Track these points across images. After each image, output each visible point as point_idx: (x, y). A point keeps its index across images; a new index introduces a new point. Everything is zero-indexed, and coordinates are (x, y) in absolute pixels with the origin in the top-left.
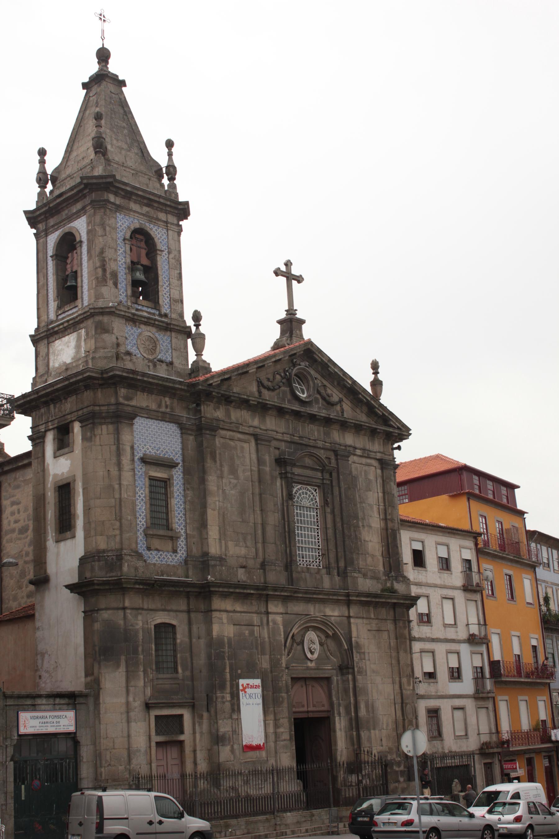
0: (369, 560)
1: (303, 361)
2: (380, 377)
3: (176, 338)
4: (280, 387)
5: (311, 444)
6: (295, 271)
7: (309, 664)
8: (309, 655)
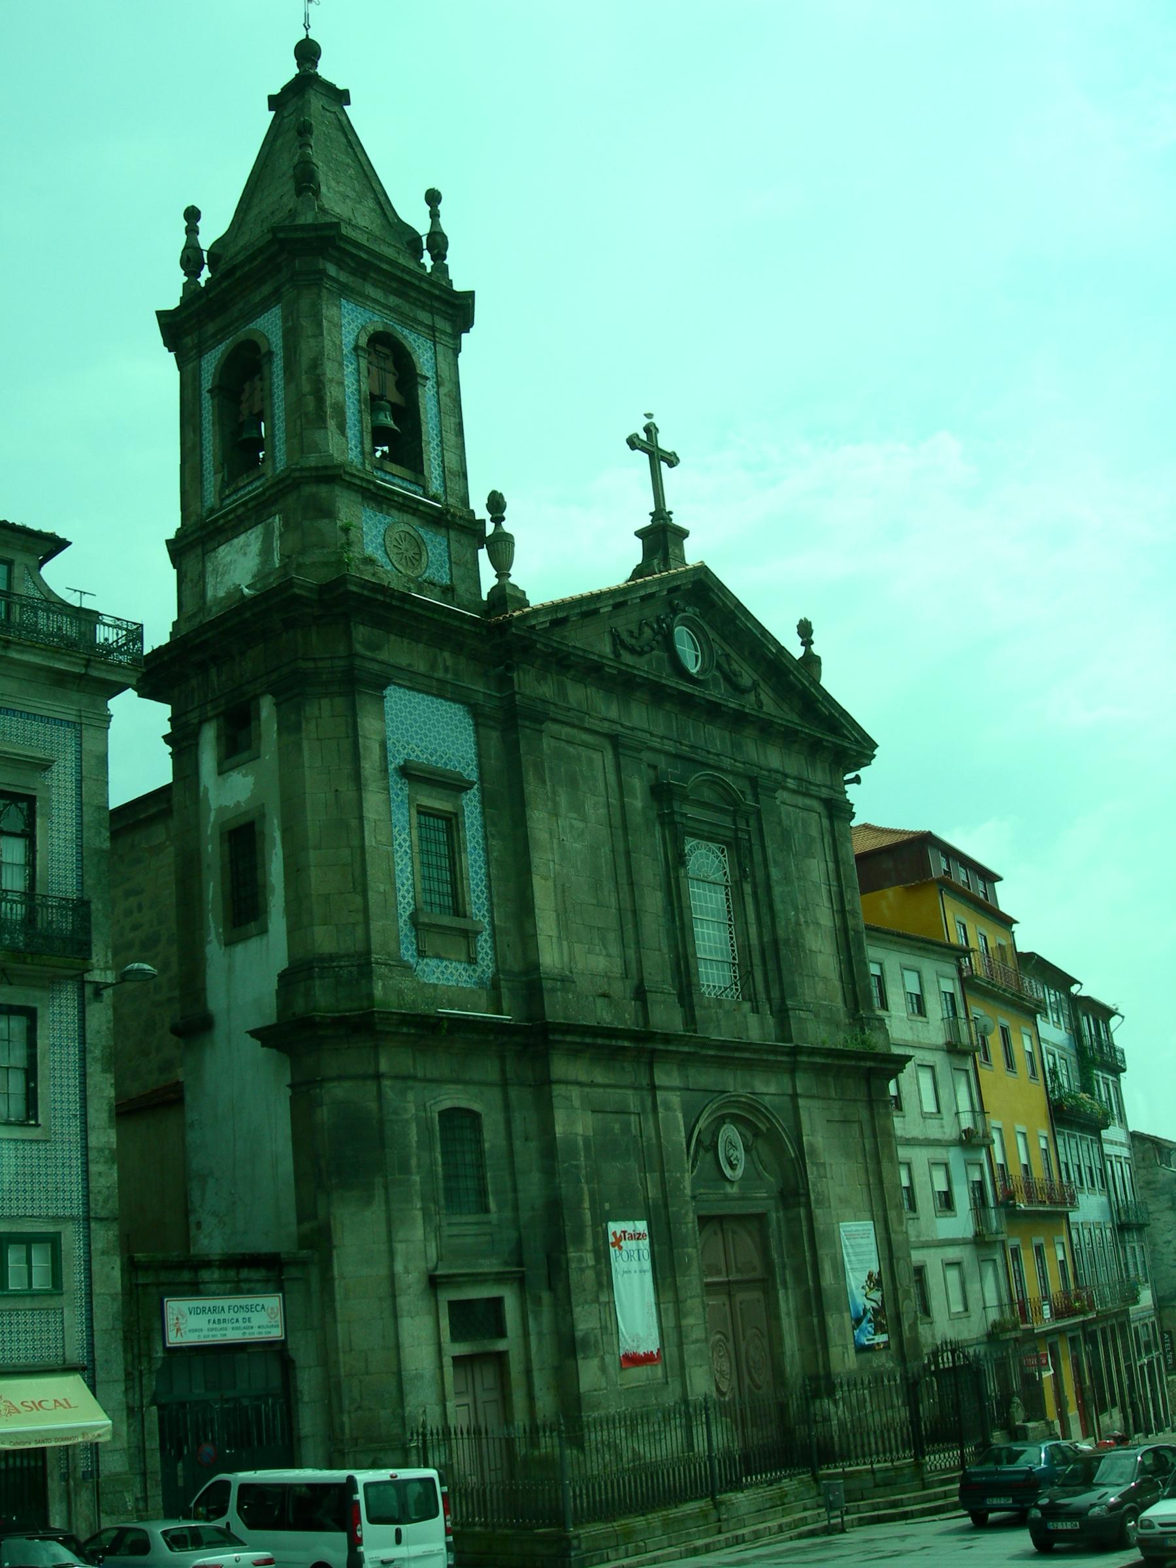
0: (820, 986)
1: (689, 605)
2: (815, 649)
3: (458, 541)
4: (652, 649)
5: (712, 762)
6: (665, 443)
8: (728, 1172)
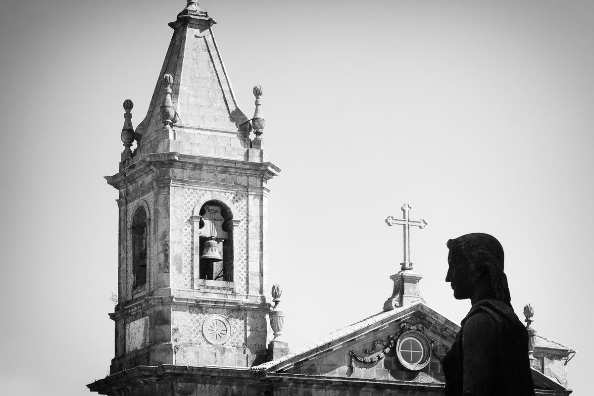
3: (253, 317)
6: (413, 215)
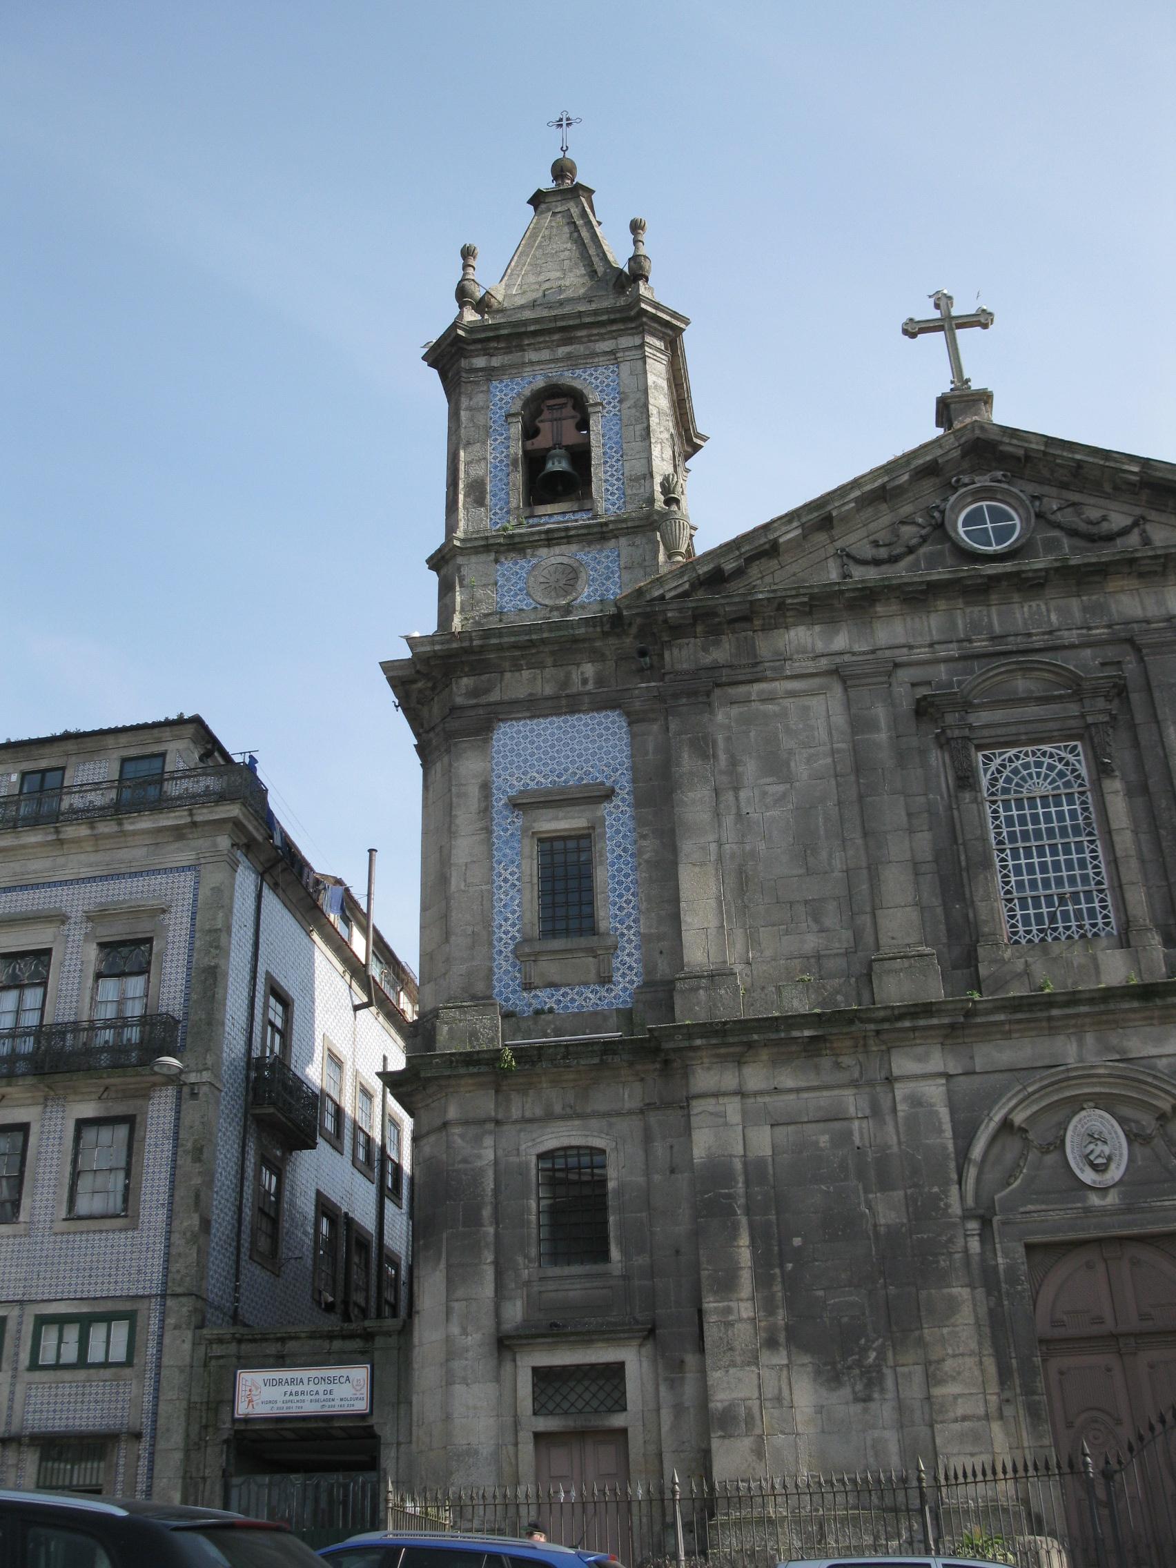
5: (1037, 645)
7: (1094, 1200)
8: (1088, 1176)
